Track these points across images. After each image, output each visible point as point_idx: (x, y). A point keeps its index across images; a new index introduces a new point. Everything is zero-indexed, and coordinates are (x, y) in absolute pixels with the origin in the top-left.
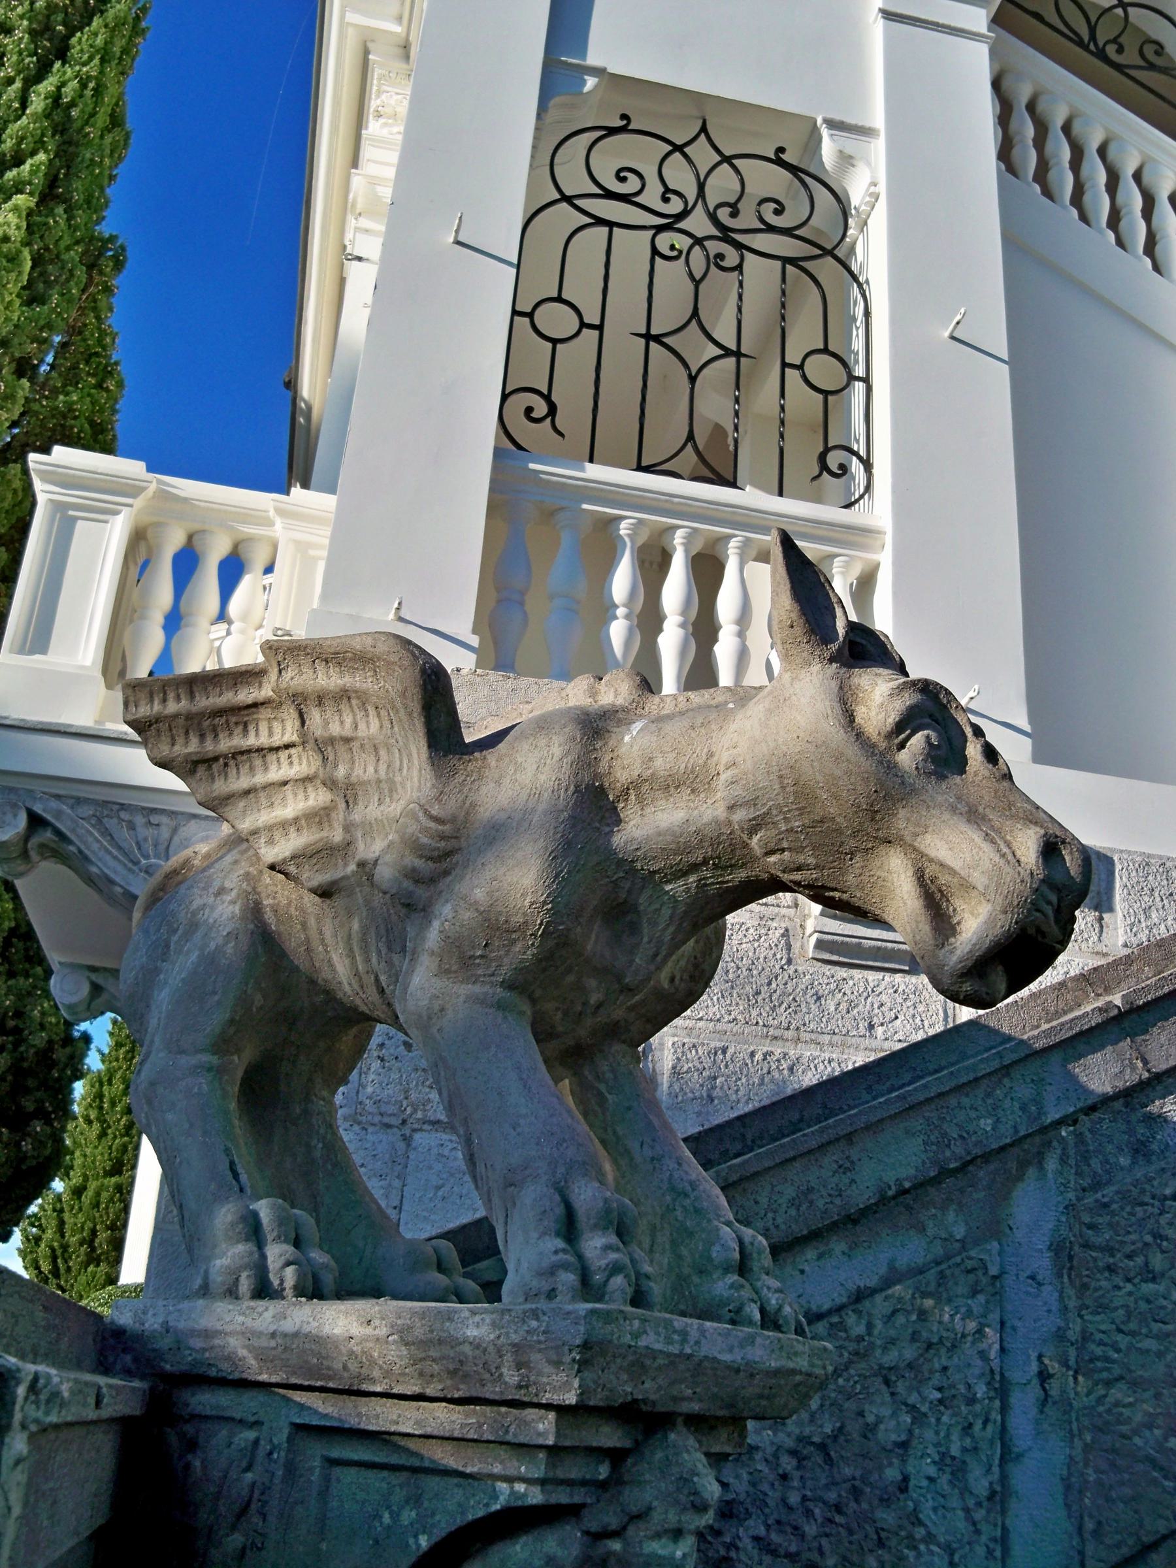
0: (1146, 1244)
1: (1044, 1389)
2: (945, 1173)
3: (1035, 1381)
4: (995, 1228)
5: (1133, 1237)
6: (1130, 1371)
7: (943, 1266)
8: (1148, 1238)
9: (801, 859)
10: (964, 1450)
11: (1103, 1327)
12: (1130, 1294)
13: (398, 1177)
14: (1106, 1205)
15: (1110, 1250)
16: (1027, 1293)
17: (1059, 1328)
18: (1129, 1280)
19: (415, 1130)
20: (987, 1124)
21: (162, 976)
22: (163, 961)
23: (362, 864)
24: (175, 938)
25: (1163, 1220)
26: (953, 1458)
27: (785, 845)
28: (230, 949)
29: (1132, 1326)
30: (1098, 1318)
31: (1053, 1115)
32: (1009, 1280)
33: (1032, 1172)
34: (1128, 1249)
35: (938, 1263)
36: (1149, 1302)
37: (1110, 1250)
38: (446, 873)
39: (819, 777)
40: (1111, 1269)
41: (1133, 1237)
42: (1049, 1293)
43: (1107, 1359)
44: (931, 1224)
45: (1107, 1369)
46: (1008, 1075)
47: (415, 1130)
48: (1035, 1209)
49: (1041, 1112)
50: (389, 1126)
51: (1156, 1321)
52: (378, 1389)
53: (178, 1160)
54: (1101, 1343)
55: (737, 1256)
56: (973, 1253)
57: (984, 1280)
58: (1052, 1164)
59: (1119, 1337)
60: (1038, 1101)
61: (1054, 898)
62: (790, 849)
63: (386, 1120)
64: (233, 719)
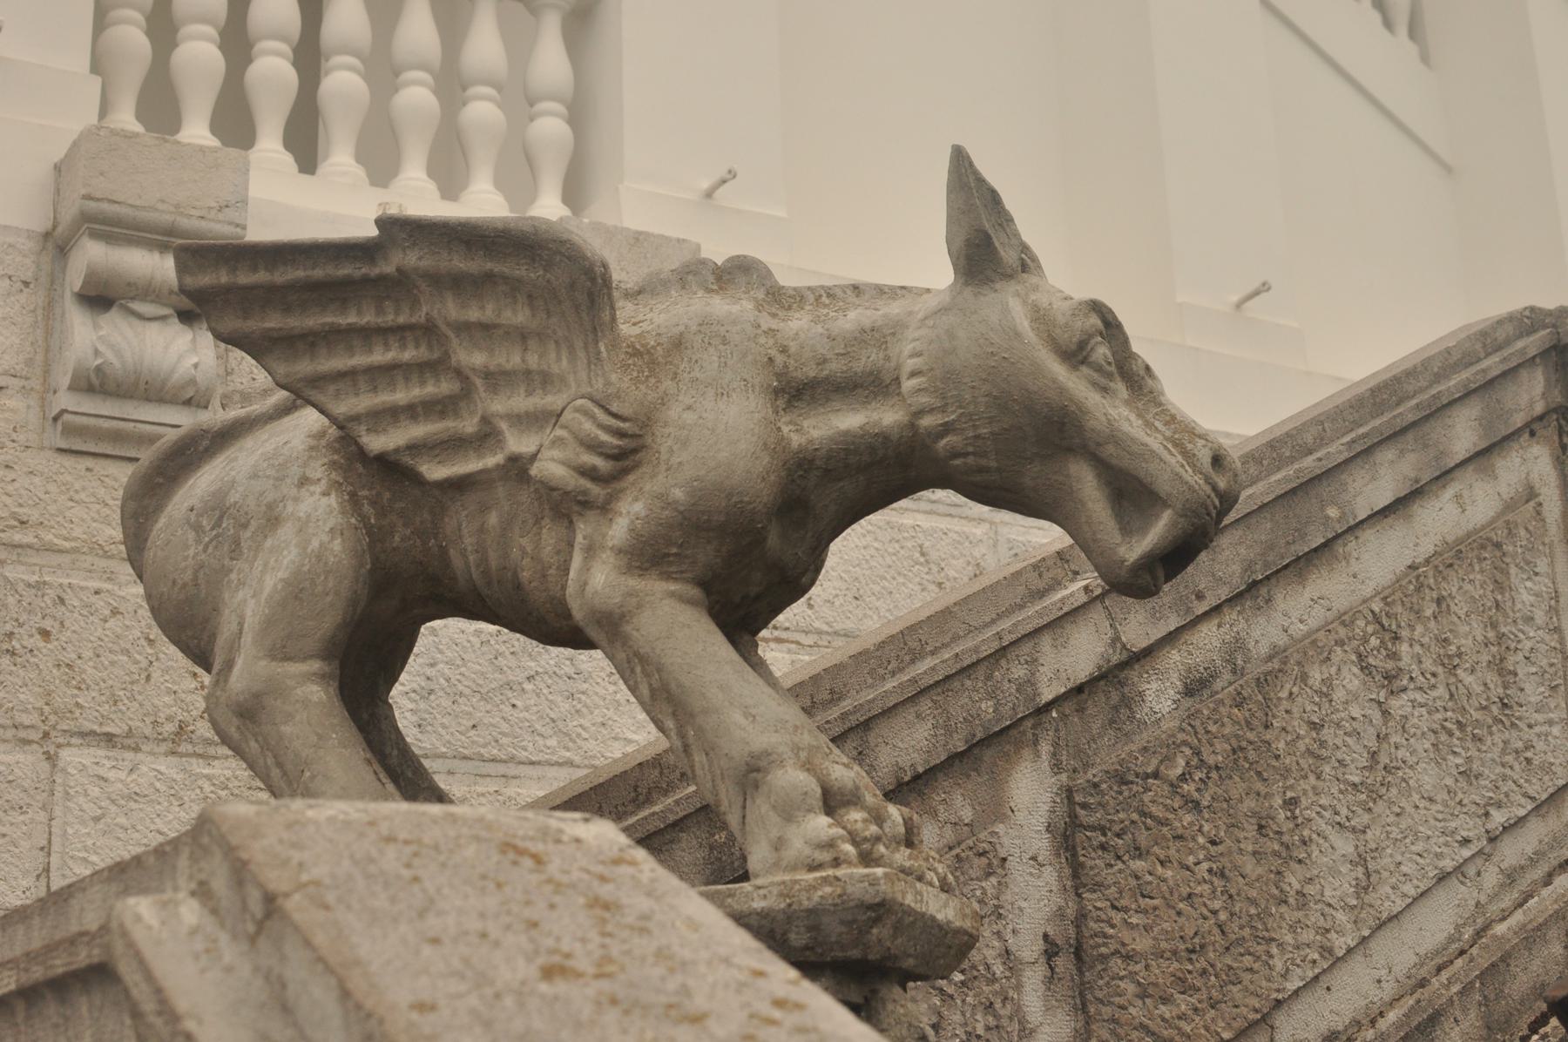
0: (1133, 822)
1: (1052, 969)
2: (955, 758)
3: (1042, 960)
4: (997, 810)
5: (1122, 815)
6: (1124, 945)
7: (957, 851)
8: (1135, 816)
9: (984, 462)
10: (988, 1028)
11: (1099, 904)
12: (1120, 871)
13: (44, 808)
14: (1096, 786)
16: (1031, 874)
17: (1060, 908)
18: (1119, 858)
19: (59, 746)
20: (988, 706)
21: (233, 576)
22: (232, 559)
23: (514, 459)
24: (248, 534)
25: (1147, 797)
26: (978, 1037)
27: (971, 449)
28: (337, 545)
29: (1123, 902)
30: (1094, 896)
31: (1047, 695)
32: (1012, 863)
33: (1027, 753)
34: (1117, 828)
35: (951, 848)
36: (1137, 878)
38: (625, 471)
40: (1103, 847)
41: (1122, 815)
42: (1050, 875)
43: (1105, 936)
44: (941, 808)
45: (1105, 944)
46: (1004, 656)
47: (59, 746)
48: (1031, 790)
49: (1036, 694)
50: (30, 742)
51: (1144, 896)
53: (307, 774)
54: (1099, 920)
55: (902, 830)
56: (982, 836)
57: (995, 862)
58: (1045, 748)
59: (1113, 913)
60: (1031, 682)
61: (1217, 502)
62: (973, 454)
63: (22, 734)
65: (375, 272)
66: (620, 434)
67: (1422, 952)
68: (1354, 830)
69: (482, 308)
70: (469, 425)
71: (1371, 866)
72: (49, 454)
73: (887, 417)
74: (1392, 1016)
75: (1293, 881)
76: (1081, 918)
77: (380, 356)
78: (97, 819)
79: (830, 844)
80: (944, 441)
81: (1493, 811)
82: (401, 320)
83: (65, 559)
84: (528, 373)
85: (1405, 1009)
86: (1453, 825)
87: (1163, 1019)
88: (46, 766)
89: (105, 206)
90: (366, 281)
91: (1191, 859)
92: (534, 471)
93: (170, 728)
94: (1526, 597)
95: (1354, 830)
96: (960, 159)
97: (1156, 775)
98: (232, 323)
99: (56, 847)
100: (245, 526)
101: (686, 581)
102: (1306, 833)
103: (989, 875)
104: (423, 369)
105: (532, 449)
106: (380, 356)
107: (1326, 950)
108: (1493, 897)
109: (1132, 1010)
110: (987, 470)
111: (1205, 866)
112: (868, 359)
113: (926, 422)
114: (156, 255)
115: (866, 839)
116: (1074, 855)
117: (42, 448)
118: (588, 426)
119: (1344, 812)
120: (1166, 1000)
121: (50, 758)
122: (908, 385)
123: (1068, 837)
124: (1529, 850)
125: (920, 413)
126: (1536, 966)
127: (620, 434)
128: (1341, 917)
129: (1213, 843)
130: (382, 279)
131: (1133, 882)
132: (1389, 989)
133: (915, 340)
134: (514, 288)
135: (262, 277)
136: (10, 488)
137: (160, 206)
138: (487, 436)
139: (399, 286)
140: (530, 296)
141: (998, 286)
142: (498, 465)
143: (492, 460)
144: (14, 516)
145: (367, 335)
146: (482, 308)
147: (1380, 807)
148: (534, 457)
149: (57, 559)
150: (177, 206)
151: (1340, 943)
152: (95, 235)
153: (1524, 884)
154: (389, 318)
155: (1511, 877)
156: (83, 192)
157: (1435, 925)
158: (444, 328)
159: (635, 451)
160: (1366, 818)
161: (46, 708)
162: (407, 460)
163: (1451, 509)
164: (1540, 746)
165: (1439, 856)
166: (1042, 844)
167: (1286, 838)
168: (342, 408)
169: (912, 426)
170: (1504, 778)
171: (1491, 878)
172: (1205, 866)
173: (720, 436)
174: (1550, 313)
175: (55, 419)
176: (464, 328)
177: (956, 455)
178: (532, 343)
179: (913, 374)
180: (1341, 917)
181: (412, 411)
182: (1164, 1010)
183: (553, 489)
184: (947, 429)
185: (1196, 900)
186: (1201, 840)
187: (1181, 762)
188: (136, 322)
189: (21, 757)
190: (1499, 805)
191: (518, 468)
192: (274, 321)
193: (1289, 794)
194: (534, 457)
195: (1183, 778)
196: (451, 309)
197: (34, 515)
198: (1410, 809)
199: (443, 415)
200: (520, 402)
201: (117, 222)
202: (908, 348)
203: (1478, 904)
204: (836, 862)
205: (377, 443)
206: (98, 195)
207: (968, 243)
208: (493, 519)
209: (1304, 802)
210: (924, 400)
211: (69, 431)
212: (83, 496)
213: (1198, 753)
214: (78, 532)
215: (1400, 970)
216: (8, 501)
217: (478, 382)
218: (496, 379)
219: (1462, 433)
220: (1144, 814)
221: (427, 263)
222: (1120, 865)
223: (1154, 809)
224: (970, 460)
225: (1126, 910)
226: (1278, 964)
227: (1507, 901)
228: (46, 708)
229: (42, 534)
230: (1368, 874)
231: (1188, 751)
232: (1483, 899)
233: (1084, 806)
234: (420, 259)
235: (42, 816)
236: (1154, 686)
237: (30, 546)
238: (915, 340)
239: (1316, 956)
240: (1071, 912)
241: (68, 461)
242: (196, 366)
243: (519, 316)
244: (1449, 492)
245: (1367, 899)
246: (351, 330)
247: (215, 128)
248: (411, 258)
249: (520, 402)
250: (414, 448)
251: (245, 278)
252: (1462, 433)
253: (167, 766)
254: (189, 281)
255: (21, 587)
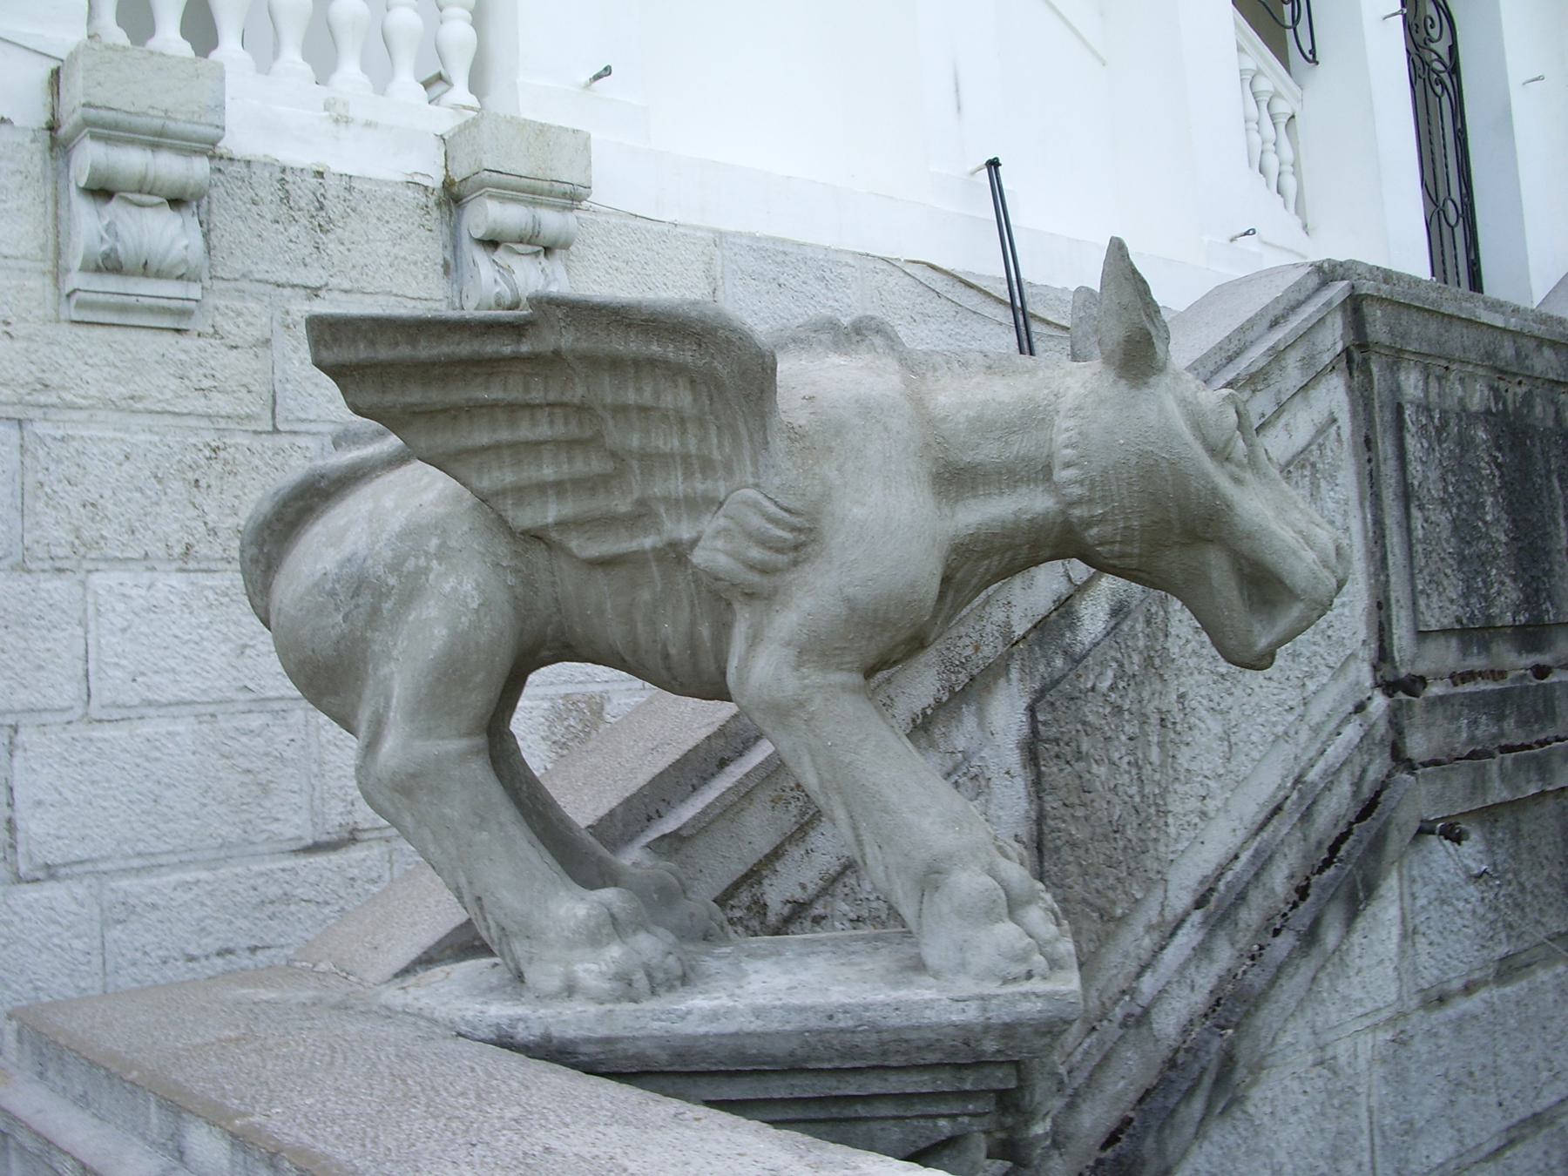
8: (1079, 727)
9: (1128, 549)
15: (1057, 741)
19: (89, 571)
31: (1019, 631)
33: (1002, 681)
34: (1066, 738)
37: (1057, 741)
38: (795, 563)
39: (1170, 489)
40: (1057, 756)
47: (89, 571)
52: (826, 1065)
58: (1015, 674)
59: (1063, 811)
60: (1008, 624)
63: (58, 564)
64: (475, 370)
65: (525, 348)
66: (793, 529)
67: (1261, 801)
68: (1221, 712)
69: (639, 390)
70: (623, 505)
71: (1233, 739)
72: (66, 327)
73: (1036, 503)
74: (1244, 857)
75: (1183, 759)
76: (1040, 819)
77: (525, 432)
78: (124, 630)
79: (1023, 957)
80: (1094, 531)
81: (1308, 683)
82: (552, 397)
83: (83, 415)
84: (686, 458)
85: (1251, 852)
86: (1283, 697)
87: (1098, 891)
88: (79, 590)
89: (103, 113)
90: (516, 358)
91: (1117, 755)
92: (699, 557)
93: (178, 550)
94: (1331, 505)
95: (1221, 712)
96: (1118, 249)
97: (1093, 689)
98: (370, 397)
99: (92, 656)
100: (388, 595)
101: (850, 670)
102: (1192, 720)
103: (979, 794)
104: (571, 444)
105: (694, 534)
106: (525, 432)
107: (1203, 814)
108: (1305, 749)
109: (1077, 888)
110: (1131, 556)
111: (1126, 759)
112: (1021, 446)
113: (1077, 512)
114: (149, 153)
115: (1048, 942)
116: (1037, 765)
117: (58, 321)
118: (756, 521)
119: (1216, 698)
120: (1098, 876)
121: (83, 583)
122: (1061, 475)
123: (1032, 750)
124: (1327, 708)
125: (1072, 504)
126: (1334, 804)
127: (793, 529)
128: (1212, 784)
129: (1131, 739)
130: (533, 359)
131: (1077, 781)
132: (1241, 834)
133: (1067, 430)
134: (674, 371)
135: (404, 351)
136: (33, 357)
137: (151, 112)
138: (641, 516)
139: (551, 363)
140: (692, 382)
141: (1152, 380)
142: (654, 549)
143: (648, 542)
144: (39, 381)
145: (513, 408)
146: (639, 390)
147: (1238, 692)
148: (694, 543)
149: (75, 415)
150: (166, 112)
151: (1211, 805)
152: (94, 137)
153: (1323, 736)
154: (536, 396)
155: (1316, 730)
156: (83, 100)
157: (1267, 782)
158: (600, 411)
159: (803, 544)
160: (1230, 700)
161: (77, 542)
162: (554, 535)
163: (1283, 436)
164: (1337, 625)
165: (1275, 724)
166: (1014, 759)
167: (1179, 727)
168: (486, 483)
169: (1063, 512)
170: (1315, 654)
171: (1304, 735)
172: (1126, 759)
173: (888, 531)
174: (1341, 264)
175: (68, 296)
176: (621, 410)
177: (1101, 544)
178: (691, 427)
179: (1068, 465)
180: (1212, 784)
181: (559, 488)
182: (1098, 883)
183: (717, 579)
184: (1102, 520)
185: (1120, 789)
186: (1123, 738)
187: (1110, 673)
188: (134, 210)
189: (58, 583)
190: (1311, 676)
191: (676, 554)
192: (415, 395)
193: (1182, 690)
194: (694, 543)
195: (1112, 688)
196: (607, 391)
197: (54, 379)
198: (1257, 689)
199: (593, 490)
200: (676, 485)
201: (116, 126)
202: (1062, 438)
203: (1296, 758)
204: (1029, 976)
205: (527, 517)
206: (98, 103)
207: (1129, 340)
208: (645, 595)
209: (1191, 695)
210: (1076, 491)
211: (81, 305)
212: (96, 360)
213: (1121, 666)
214: (93, 391)
215: (1248, 819)
216: (33, 368)
217: (635, 464)
218: (651, 460)
219: (1292, 376)
220: (1084, 723)
221: (584, 345)
222: (1069, 769)
223: (1091, 718)
224: (1117, 547)
225: (1073, 806)
226: (1172, 830)
227: (1312, 753)
228: (77, 542)
229: (63, 394)
230: (1230, 747)
231: (1114, 665)
232: (1299, 751)
233: (1045, 723)
234: (578, 339)
235: (79, 631)
236: (1090, 611)
237: (53, 406)
238: (1067, 430)
239: (1197, 820)
240: (1033, 815)
241: (82, 331)
242: (186, 248)
243: (679, 398)
244: (1283, 421)
245: (1231, 767)
246: (493, 406)
247: (186, 32)
248: (568, 340)
249: (676, 485)
250: (562, 525)
251: (384, 353)
252: (1292, 376)
253: (178, 581)
254: (328, 356)
255: (48, 441)
